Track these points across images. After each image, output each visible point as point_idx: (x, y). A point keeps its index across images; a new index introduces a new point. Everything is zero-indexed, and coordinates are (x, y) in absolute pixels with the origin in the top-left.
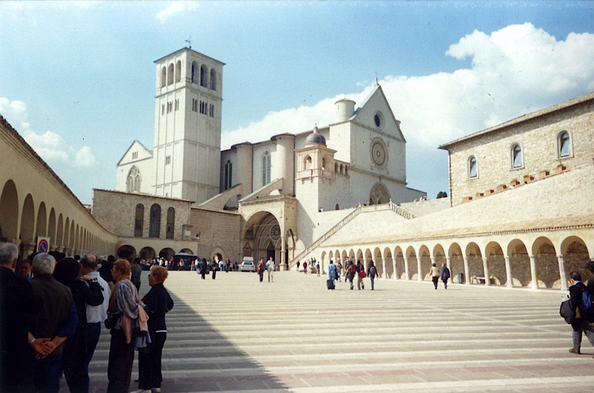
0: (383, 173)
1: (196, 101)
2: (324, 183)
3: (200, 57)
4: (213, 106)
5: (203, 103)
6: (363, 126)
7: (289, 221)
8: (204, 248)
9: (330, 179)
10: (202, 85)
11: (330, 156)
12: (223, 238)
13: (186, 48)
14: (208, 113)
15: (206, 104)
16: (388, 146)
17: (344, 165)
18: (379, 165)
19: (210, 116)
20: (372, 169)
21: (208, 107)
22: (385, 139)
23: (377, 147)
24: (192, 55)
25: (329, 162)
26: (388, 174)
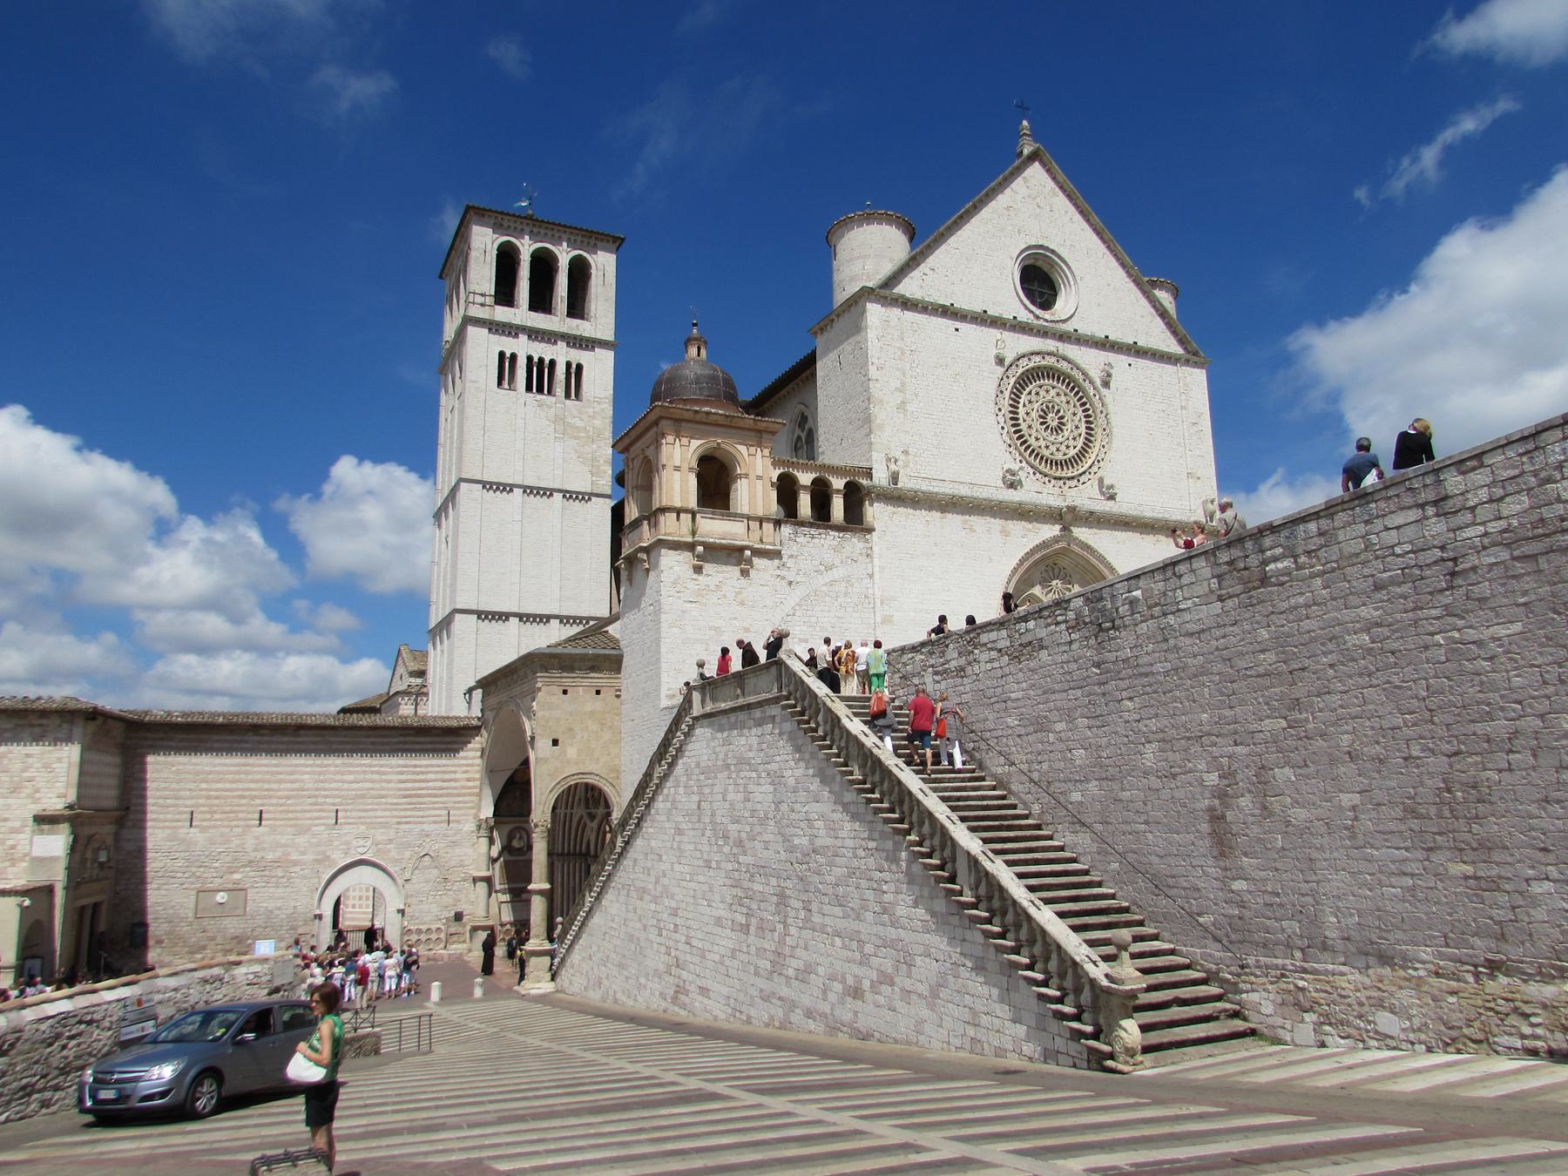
0: (1085, 496)
1: (514, 357)
2: (698, 570)
3: (527, 229)
4: (580, 367)
5: (541, 360)
6: (947, 312)
7: (572, 752)
8: (280, 873)
9: (741, 549)
10: (534, 306)
11: (742, 449)
12: (385, 825)
13: (468, 209)
14: (560, 388)
15: (553, 363)
16: (1106, 384)
17: (838, 483)
18: (1062, 467)
19: (568, 396)
20: (1012, 486)
21: (560, 370)
22: (1090, 361)
23: (1052, 392)
24: (498, 228)
25: (740, 477)
26: (1112, 497)
